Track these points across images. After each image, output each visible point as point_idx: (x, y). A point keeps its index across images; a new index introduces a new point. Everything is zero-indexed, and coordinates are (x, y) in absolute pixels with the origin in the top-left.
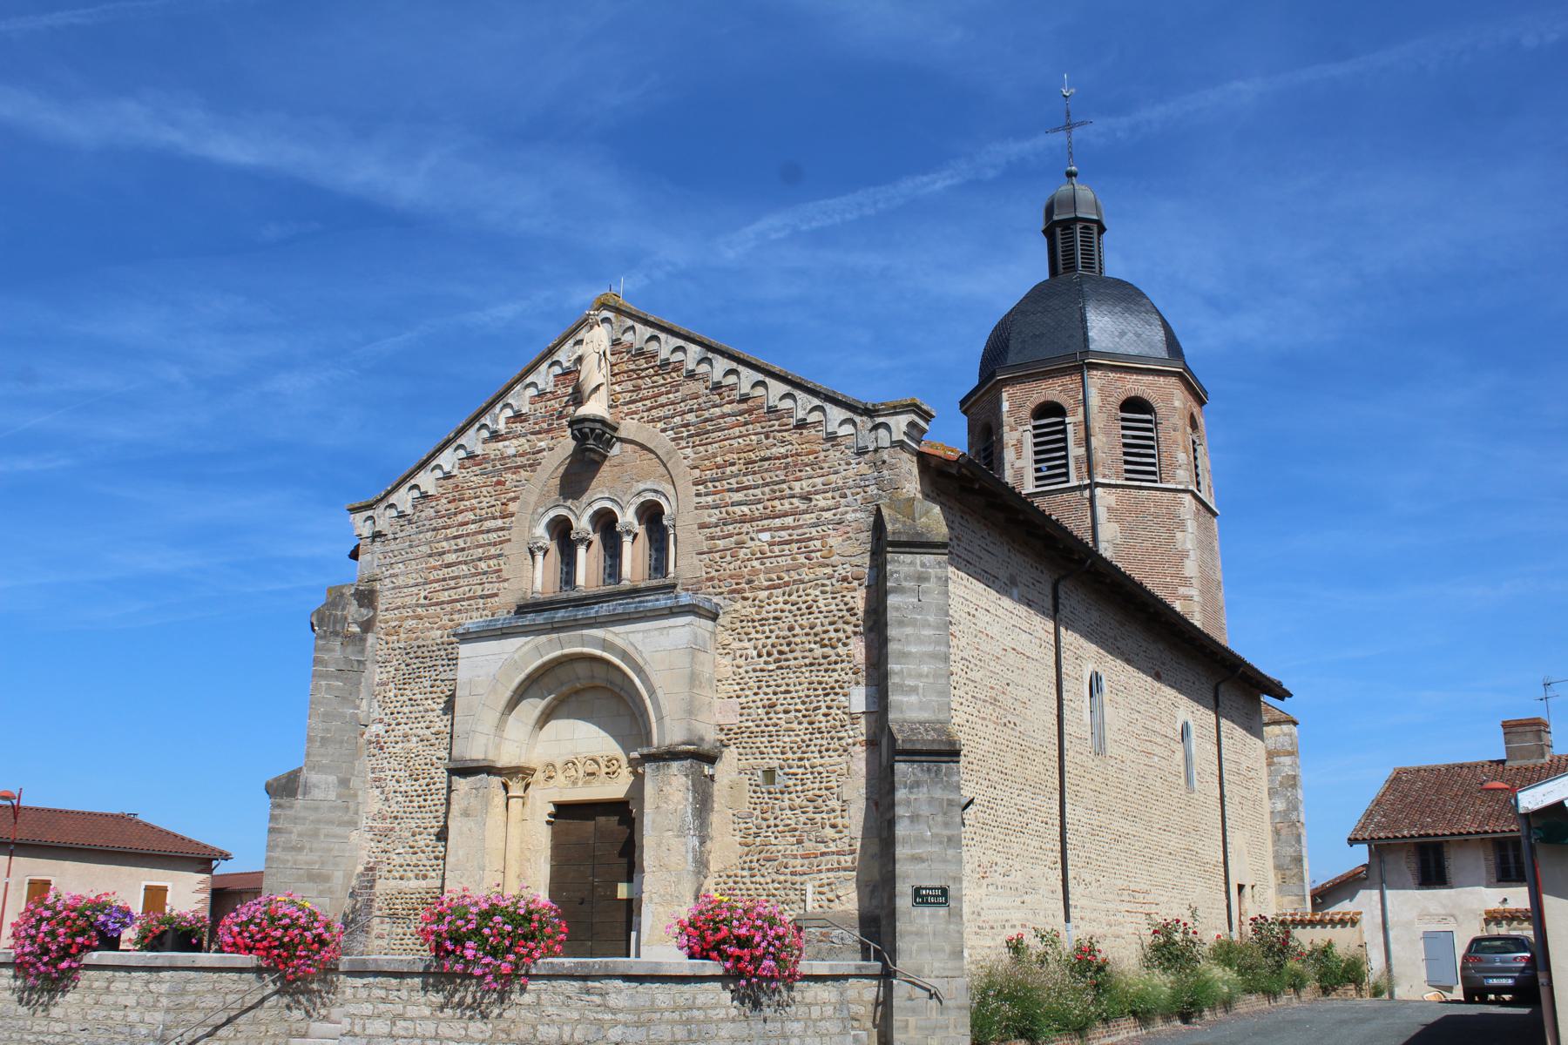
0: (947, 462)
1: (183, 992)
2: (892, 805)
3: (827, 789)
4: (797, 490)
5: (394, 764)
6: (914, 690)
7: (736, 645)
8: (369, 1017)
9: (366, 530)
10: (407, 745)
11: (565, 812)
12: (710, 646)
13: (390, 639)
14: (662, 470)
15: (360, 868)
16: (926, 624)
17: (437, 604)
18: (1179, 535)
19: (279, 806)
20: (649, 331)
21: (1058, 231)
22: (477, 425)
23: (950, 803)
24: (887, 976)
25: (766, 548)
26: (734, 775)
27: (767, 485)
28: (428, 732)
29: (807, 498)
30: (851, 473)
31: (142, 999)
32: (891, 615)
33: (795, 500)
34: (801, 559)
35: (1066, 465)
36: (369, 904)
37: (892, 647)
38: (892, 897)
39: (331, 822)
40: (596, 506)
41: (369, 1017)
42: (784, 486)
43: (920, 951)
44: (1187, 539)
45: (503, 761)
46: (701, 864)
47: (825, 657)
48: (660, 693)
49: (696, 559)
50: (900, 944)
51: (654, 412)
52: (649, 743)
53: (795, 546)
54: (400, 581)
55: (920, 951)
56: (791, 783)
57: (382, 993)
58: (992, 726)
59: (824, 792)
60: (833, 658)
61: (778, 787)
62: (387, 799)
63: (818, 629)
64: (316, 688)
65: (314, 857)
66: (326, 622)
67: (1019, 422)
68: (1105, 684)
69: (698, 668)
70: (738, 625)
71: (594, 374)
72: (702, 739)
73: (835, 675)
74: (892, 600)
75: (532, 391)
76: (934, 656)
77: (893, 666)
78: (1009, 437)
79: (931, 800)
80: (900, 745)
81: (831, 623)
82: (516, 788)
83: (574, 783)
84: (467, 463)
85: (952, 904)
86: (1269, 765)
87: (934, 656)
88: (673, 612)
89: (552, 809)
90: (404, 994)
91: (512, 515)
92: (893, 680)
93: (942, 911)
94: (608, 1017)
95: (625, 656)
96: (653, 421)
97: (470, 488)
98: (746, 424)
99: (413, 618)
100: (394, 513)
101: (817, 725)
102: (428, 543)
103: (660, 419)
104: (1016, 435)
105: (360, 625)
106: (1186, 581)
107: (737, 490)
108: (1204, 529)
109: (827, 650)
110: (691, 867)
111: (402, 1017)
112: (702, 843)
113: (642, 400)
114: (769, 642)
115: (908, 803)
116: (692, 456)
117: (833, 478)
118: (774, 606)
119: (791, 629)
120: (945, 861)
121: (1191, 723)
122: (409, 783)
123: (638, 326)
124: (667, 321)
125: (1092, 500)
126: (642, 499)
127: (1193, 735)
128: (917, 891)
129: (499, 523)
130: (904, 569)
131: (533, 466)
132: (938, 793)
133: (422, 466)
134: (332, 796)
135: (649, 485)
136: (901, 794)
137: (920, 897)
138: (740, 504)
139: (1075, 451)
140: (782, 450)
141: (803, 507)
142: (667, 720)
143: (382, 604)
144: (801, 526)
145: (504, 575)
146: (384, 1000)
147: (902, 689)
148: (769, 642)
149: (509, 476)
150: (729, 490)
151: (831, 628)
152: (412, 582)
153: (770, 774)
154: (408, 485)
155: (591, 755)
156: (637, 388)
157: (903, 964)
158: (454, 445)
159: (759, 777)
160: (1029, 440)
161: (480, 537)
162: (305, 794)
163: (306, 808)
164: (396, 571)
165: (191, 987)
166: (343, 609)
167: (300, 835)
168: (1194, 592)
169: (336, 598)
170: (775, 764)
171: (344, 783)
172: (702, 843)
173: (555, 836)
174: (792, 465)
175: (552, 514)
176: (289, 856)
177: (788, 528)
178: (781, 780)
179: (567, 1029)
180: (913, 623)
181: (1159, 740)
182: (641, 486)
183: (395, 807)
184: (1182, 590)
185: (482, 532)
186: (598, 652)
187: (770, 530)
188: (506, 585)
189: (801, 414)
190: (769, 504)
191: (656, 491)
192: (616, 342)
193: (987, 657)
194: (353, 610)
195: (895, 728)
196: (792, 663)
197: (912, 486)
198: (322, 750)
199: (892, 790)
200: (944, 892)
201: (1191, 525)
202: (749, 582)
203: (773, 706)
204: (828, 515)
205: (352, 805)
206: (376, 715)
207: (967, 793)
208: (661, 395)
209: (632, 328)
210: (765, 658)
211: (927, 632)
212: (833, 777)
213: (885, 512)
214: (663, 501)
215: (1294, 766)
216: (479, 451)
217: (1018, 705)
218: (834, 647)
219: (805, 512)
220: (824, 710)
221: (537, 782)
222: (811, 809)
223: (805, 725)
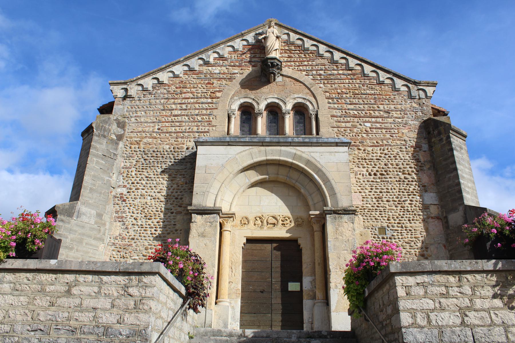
3: (415, 238)
7: (356, 169)
8: (432, 311)
10: (143, 201)
13: (133, 146)
14: (307, 91)
17: (167, 133)
20: (298, 36)
22: (197, 58)
25: (369, 129)
26: (362, 229)
27: (366, 104)
28: (159, 195)
29: (388, 112)
30: (408, 106)
31: (117, 302)
32: (456, 159)
33: (381, 112)
34: (388, 136)
39: (90, 237)
40: (269, 101)
41: (432, 311)
42: (375, 106)
47: (405, 178)
48: (333, 182)
49: (331, 129)
51: (301, 67)
52: (326, 205)
53: (384, 131)
54: (142, 120)
56: (395, 234)
57: (443, 290)
59: (414, 239)
60: (411, 180)
62: (127, 228)
63: (402, 166)
70: (356, 160)
73: (413, 187)
74: (455, 153)
81: (407, 164)
82: (228, 226)
84: (188, 73)
88: (337, 144)
89: (245, 241)
90: (467, 290)
91: (218, 98)
92: (462, 187)
95: (308, 162)
96: (301, 70)
97: (190, 83)
98: (351, 79)
99: (150, 138)
100: (140, 88)
101: (406, 208)
102: (163, 104)
103: (304, 70)
107: (350, 104)
109: (407, 176)
113: (293, 61)
114: (375, 170)
116: (324, 87)
117: (399, 106)
118: (375, 155)
122: (144, 221)
123: (291, 34)
126: (296, 101)
129: (210, 100)
131: (231, 79)
133: (162, 70)
134: (92, 222)
135: (300, 96)
140: (372, 92)
141: (385, 115)
142: (338, 195)
143: (128, 129)
144: (387, 123)
145: (214, 123)
148: (375, 170)
149: (215, 81)
150: (346, 103)
151: (408, 166)
152: (150, 121)
154: (151, 77)
155: (272, 214)
158: (182, 64)
161: (197, 106)
162: (77, 217)
164: (139, 114)
166: (109, 125)
167: (72, 240)
170: (385, 225)
171: (99, 216)
173: (244, 255)
174: (378, 99)
175: (242, 101)
177: (380, 123)
182: (296, 96)
183: (132, 233)
185: (199, 103)
186: (290, 160)
187: (370, 122)
188: (214, 128)
189: (381, 79)
190: (368, 112)
191: (304, 99)
196: (389, 180)
198: (90, 195)
204: (400, 120)
205: (102, 229)
206: (121, 183)
208: (304, 61)
209: (288, 34)
210: (373, 176)
212: (418, 232)
214: (308, 103)
216: (197, 68)
218: (409, 174)
220: (409, 202)
222: (408, 247)
223: (399, 208)
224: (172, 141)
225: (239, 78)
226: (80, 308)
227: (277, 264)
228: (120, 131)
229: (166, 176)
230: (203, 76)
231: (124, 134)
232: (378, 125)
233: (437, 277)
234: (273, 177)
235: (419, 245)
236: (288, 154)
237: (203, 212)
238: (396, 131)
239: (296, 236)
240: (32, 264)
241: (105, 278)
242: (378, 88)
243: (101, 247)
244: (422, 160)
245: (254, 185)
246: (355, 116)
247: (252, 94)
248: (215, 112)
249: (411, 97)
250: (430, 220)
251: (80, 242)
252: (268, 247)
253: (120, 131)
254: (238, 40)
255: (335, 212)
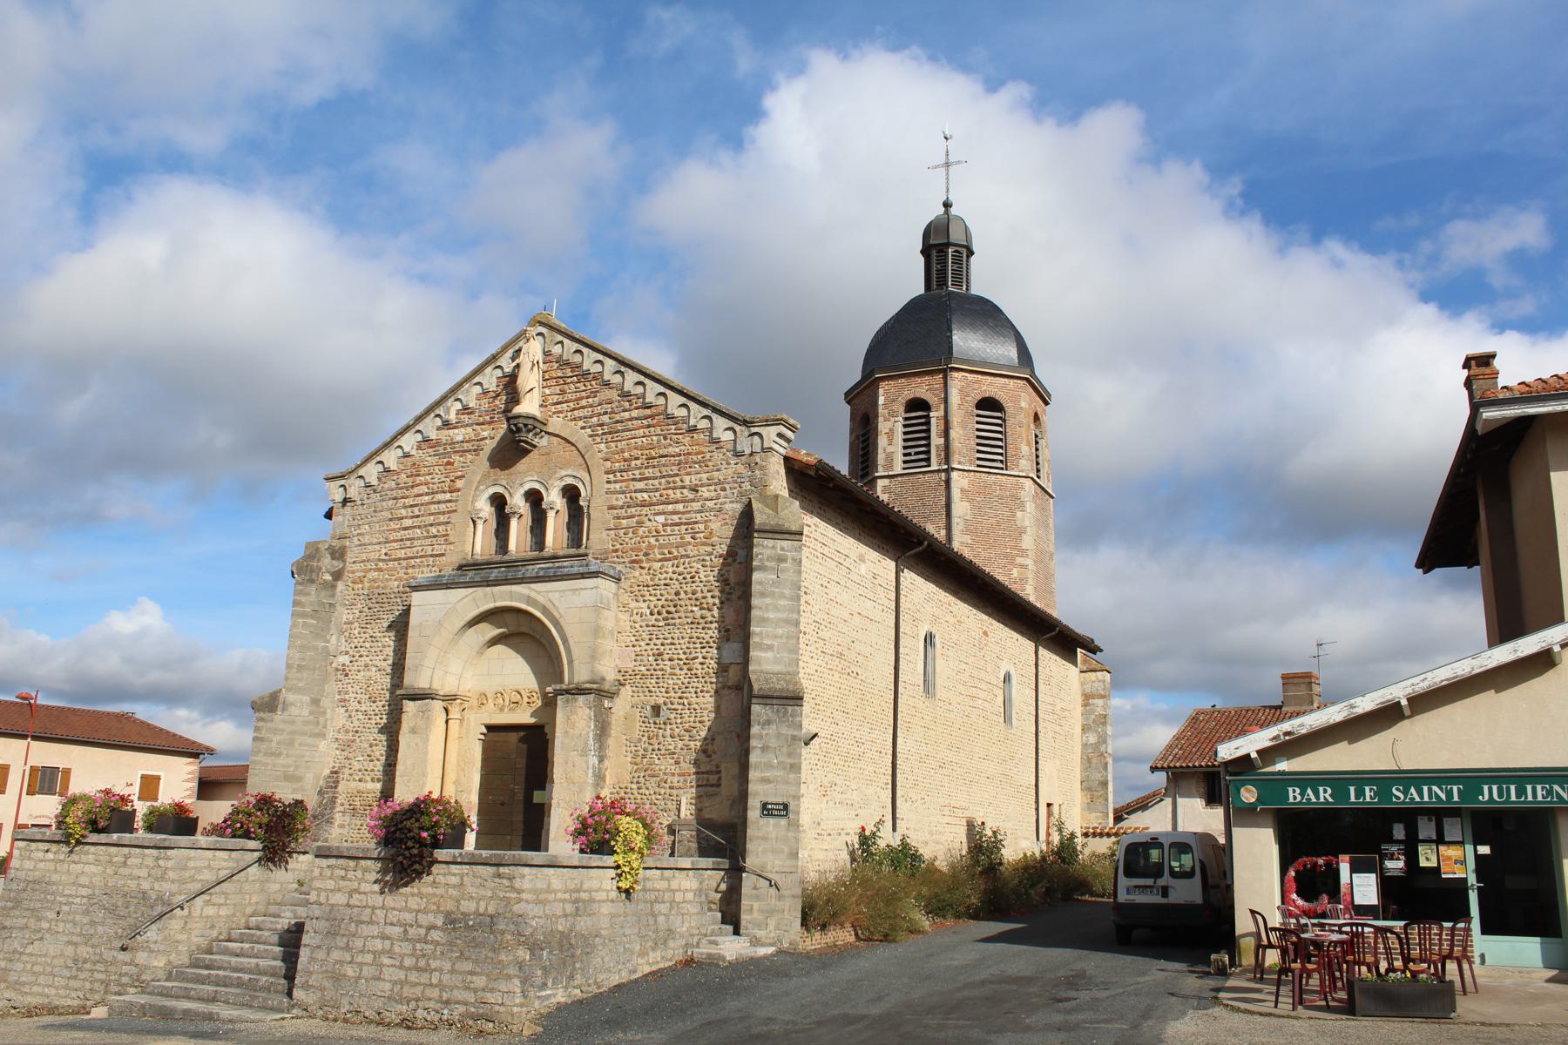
0: (807, 466)
1: (185, 868)
2: (748, 738)
4: (687, 483)
5: (356, 688)
6: (770, 648)
7: (633, 604)
9: (339, 497)
11: (491, 728)
12: (613, 605)
14: (581, 460)
15: (327, 772)
16: (783, 596)
18: (1019, 514)
19: (262, 719)
20: (576, 346)
21: (934, 253)
23: (794, 738)
24: (736, 871)
28: (384, 664)
30: (730, 471)
32: (755, 588)
34: (688, 538)
35: (928, 452)
36: (333, 801)
37: (754, 613)
38: (745, 809)
39: (304, 734)
40: (527, 487)
43: (765, 851)
44: (1027, 517)
45: (445, 685)
46: (600, 778)
50: (749, 846)
52: (561, 681)
54: (366, 539)
55: (765, 851)
57: (342, 873)
58: (837, 675)
61: (662, 719)
63: (699, 595)
64: (294, 625)
65: (290, 761)
66: (304, 570)
67: (892, 414)
68: (937, 641)
69: (602, 622)
71: (529, 380)
72: (603, 679)
74: (756, 576)
75: (478, 389)
76: (787, 621)
77: (754, 629)
78: (883, 426)
79: (779, 735)
80: (756, 691)
82: (455, 713)
83: (502, 710)
85: (791, 816)
86: (1085, 705)
87: (787, 621)
88: (583, 576)
90: (359, 874)
92: (754, 640)
93: (783, 822)
94: (514, 895)
95: (545, 610)
104: (889, 424)
105: (332, 574)
106: (1023, 553)
108: (1042, 509)
110: (591, 780)
111: (357, 891)
112: (601, 761)
115: (761, 737)
117: (716, 474)
119: (677, 594)
120: (787, 783)
121: (1013, 673)
123: (566, 341)
124: (588, 338)
125: (948, 482)
127: (1014, 682)
128: (764, 806)
129: (448, 496)
130: (769, 552)
132: (785, 730)
133: (387, 445)
134: (306, 712)
136: (755, 730)
137: (766, 810)
138: (641, 491)
139: (937, 440)
141: (691, 496)
142: (576, 663)
143: (350, 557)
146: (343, 878)
147: (761, 647)
149: (456, 458)
153: (656, 710)
156: (563, 392)
157: (751, 861)
159: (648, 711)
160: (899, 429)
161: (433, 508)
163: (284, 722)
165: (191, 864)
168: (1029, 562)
169: (313, 552)
170: (661, 701)
171: (316, 702)
172: (601, 761)
174: (684, 461)
175: (491, 491)
176: (269, 760)
178: (664, 712)
179: (483, 904)
180: (772, 595)
181: (983, 686)
182: (564, 473)
183: (356, 723)
184: (1019, 560)
186: (523, 606)
189: (692, 422)
192: (546, 353)
193: (835, 621)
194: (327, 562)
195: (753, 677)
197: (779, 484)
199: (749, 726)
200: (786, 807)
201: (1030, 507)
202: (646, 554)
203: (660, 654)
204: (710, 504)
205: (321, 720)
207: (809, 726)
211: (783, 602)
213: (755, 505)
215: (1105, 707)
216: (433, 436)
217: (860, 658)
219: (692, 501)
221: (471, 708)
224: (402, 574)
225: (489, 445)
226: (131, 877)
227: (521, 763)
228: (338, 564)
229: (392, 634)
230: (441, 450)
231: (343, 568)
232: (676, 518)
233: (341, 861)
234: (513, 629)
235: (703, 734)
236: (520, 597)
237: (414, 697)
238: (702, 527)
239: (542, 722)
240: (103, 838)
241: (147, 851)
242: (687, 440)
243: (323, 745)
244: (732, 581)
245: (494, 642)
246: (643, 505)
247: (503, 477)
248: (454, 518)
249: (737, 455)
250: (726, 692)
251: (291, 743)
252: (514, 737)
253: (338, 564)
254: (489, 370)
255: (567, 692)
